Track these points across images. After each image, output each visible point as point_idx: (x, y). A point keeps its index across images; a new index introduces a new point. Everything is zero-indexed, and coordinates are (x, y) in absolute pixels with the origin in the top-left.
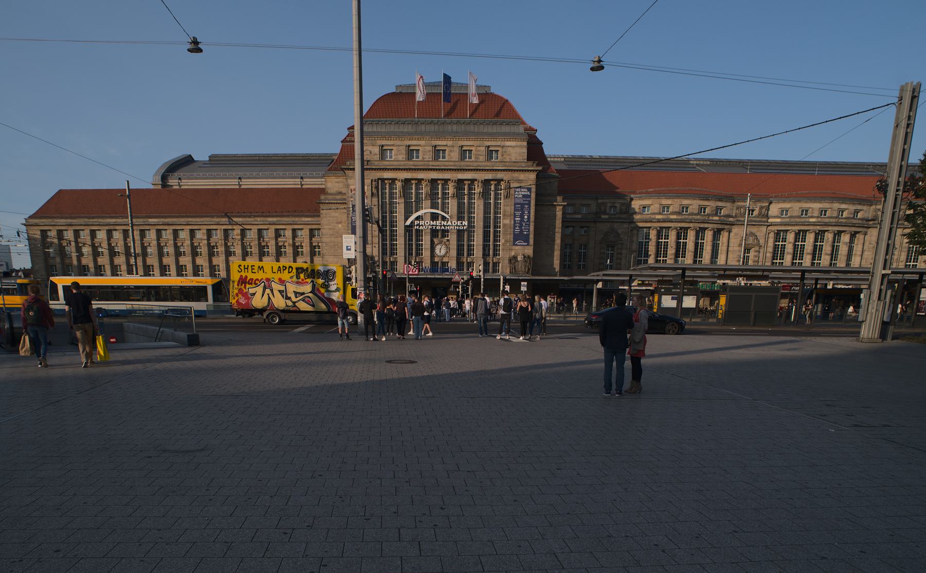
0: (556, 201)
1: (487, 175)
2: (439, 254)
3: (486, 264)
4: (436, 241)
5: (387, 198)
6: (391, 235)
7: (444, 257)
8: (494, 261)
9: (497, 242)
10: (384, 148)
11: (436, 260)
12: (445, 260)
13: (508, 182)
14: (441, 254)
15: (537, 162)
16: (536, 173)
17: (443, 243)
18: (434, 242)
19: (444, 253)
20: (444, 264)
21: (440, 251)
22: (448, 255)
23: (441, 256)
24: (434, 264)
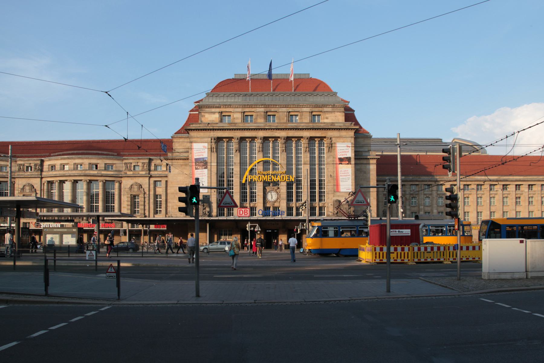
0: (370, 155)
1: (311, 133)
2: (271, 200)
3: (313, 209)
4: (268, 189)
5: (225, 154)
6: (228, 184)
7: (275, 202)
8: (320, 205)
9: (322, 189)
10: (223, 114)
11: (268, 205)
12: (276, 205)
13: (330, 139)
14: (273, 199)
15: (353, 123)
16: (354, 131)
17: (274, 190)
18: (266, 189)
19: (275, 199)
20: (276, 208)
21: (272, 197)
22: (279, 200)
23: (273, 202)
24: (266, 209)
